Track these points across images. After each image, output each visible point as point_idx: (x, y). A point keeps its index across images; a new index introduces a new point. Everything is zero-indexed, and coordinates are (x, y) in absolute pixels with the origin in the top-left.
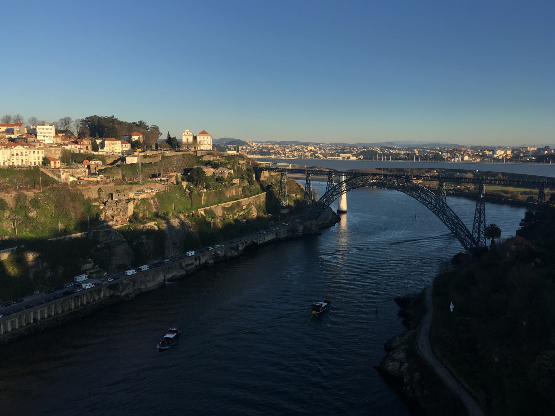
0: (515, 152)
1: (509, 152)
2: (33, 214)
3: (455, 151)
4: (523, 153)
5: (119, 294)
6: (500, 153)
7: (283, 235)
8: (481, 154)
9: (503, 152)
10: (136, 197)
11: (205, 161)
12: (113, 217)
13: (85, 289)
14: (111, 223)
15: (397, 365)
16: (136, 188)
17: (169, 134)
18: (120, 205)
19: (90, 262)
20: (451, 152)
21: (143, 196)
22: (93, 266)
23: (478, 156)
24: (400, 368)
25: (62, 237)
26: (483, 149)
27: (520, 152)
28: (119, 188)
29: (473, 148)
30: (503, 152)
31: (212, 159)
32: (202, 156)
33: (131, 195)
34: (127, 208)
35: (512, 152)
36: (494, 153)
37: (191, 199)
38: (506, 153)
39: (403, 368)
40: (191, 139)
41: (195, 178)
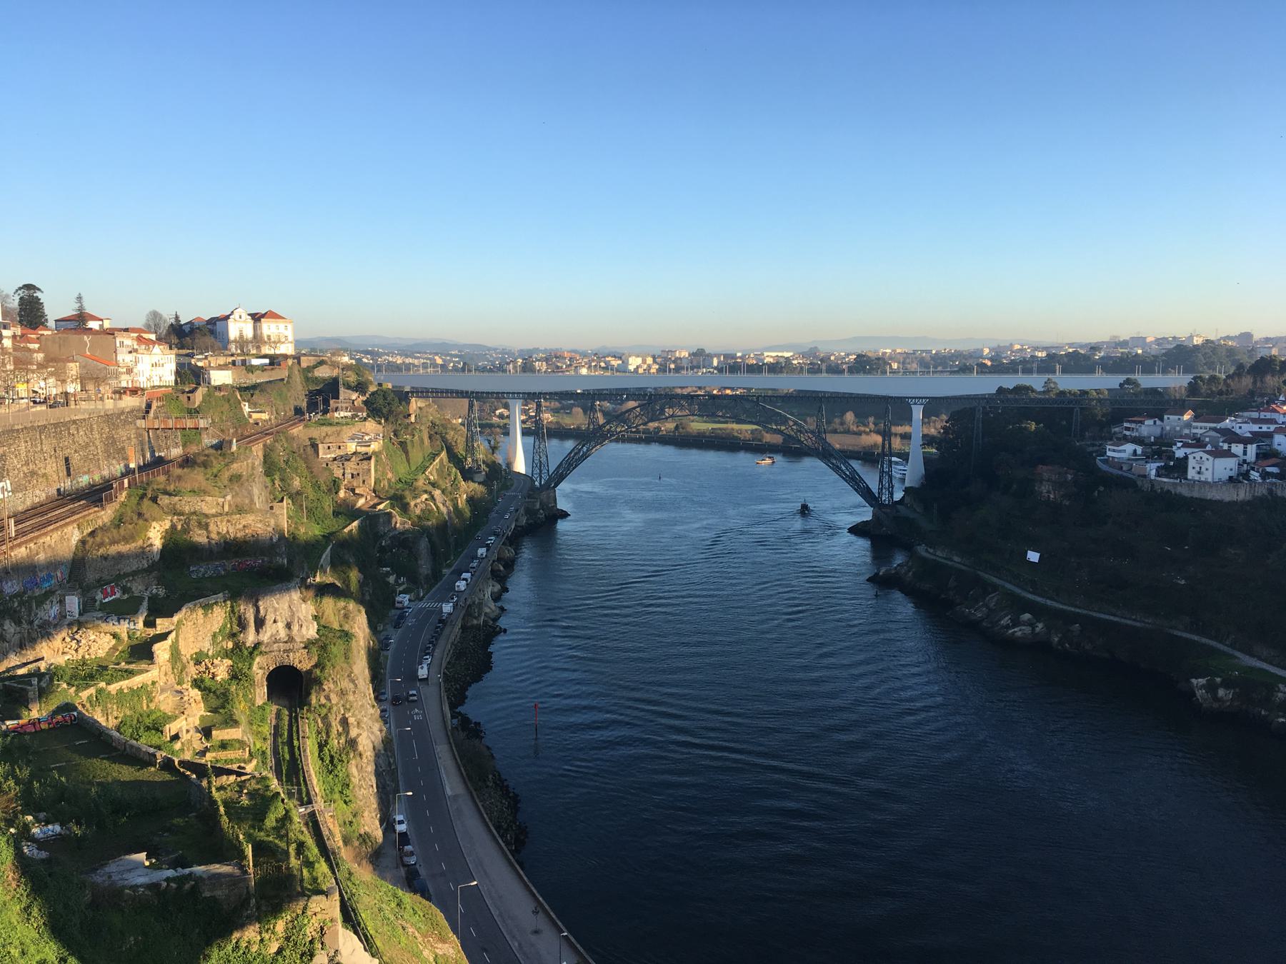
0: (659, 360)
1: (650, 361)
2: (297, 483)
3: (552, 358)
4: (674, 362)
5: (475, 622)
6: (634, 362)
7: (523, 521)
8: (603, 364)
9: (639, 361)
10: (363, 450)
11: (324, 380)
12: (353, 490)
13: (450, 614)
14: (361, 502)
15: (1027, 630)
16: (348, 432)
17: (177, 318)
18: (351, 467)
19: (388, 574)
20: (547, 360)
21: (375, 446)
22: (396, 581)
23: (606, 369)
24: (1033, 629)
25: (349, 528)
26: (599, 356)
27: (666, 359)
28: (316, 433)
29: (584, 355)
30: (639, 361)
31: (335, 373)
32: (310, 369)
33: (352, 447)
34: (369, 470)
35: (655, 362)
36: (625, 363)
37: (406, 453)
38: (644, 361)
39: (1037, 630)
40: (249, 334)
41: (385, 410)
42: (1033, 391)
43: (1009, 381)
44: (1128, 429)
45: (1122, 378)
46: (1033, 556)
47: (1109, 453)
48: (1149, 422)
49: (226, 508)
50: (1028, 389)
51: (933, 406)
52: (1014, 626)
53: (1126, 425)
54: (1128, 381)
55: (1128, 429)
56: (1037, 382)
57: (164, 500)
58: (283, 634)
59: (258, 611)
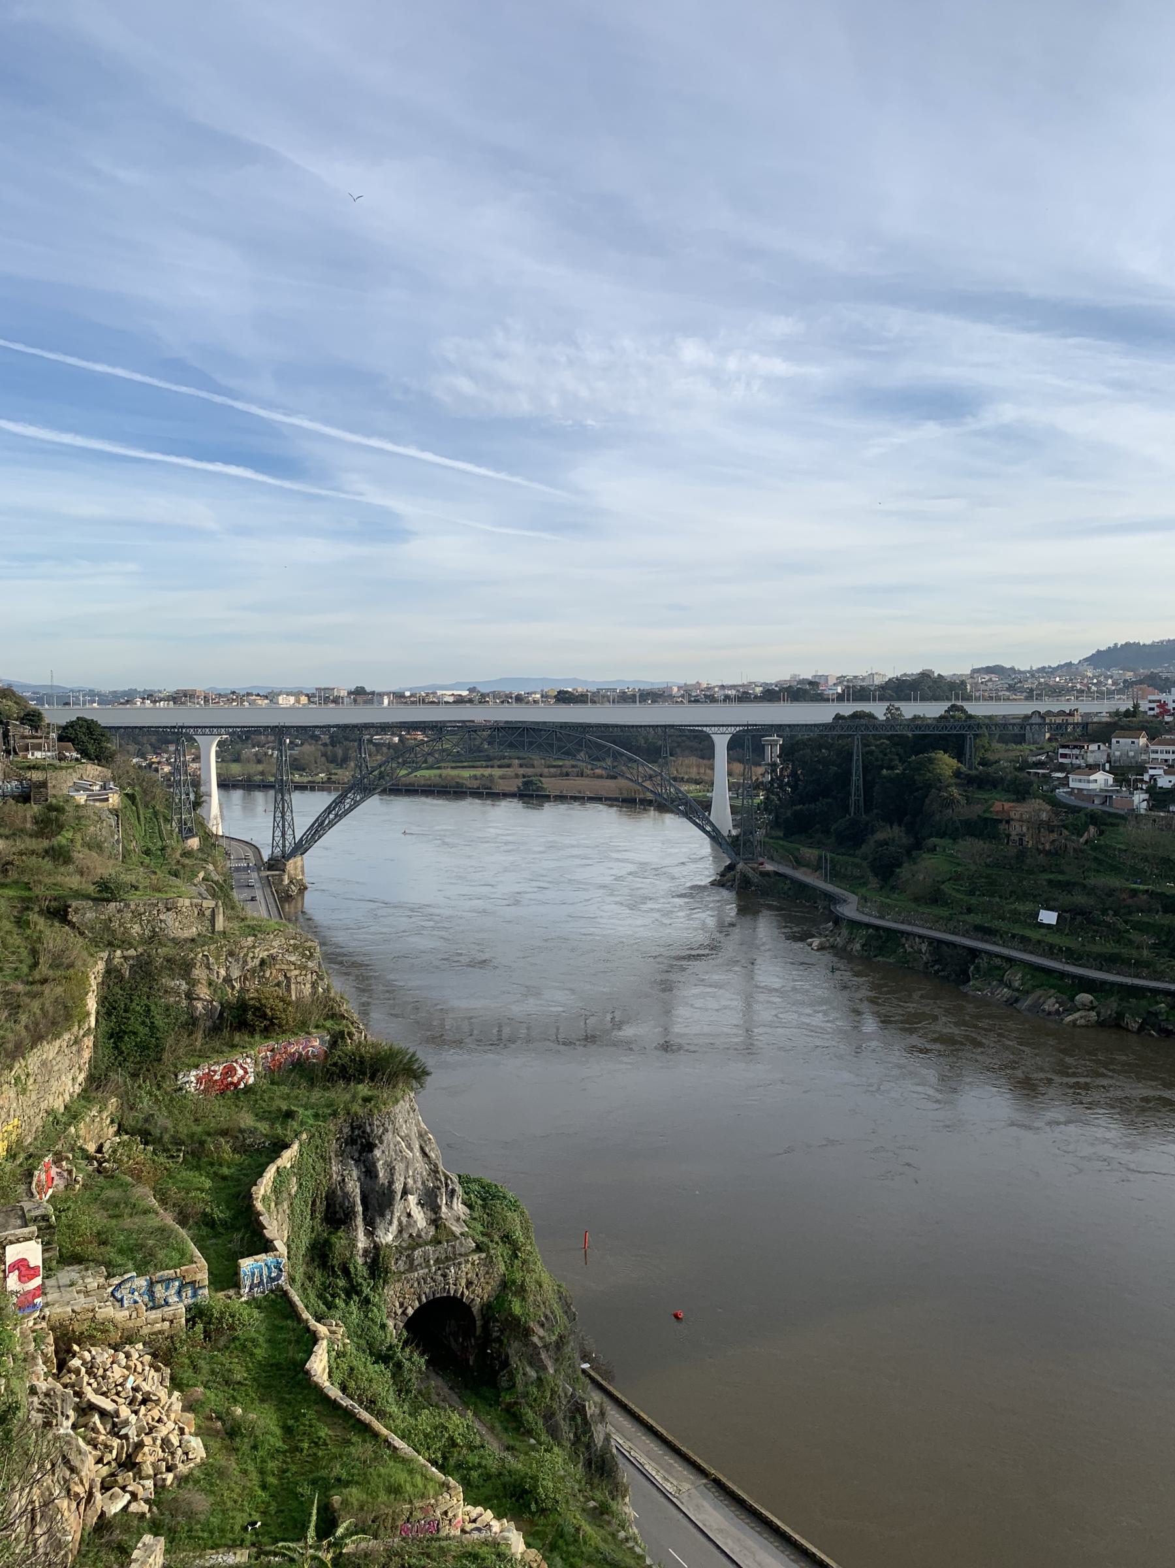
42: (876, 718)
43: (847, 709)
44: (1064, 756)
45: (946, 705)
46: (1048, 917)
47: (1072, 785)
48: (1093, 747)
49: (220, 924)
50: (871, 716)
51: (747, 743)
52: (1069, 1011)
53: (1061, 751)
54: (953, 706)
55: (1064, 756)
56: (879, 710)
57: (86, 914)
58: (420, 1218)
59: (370, 1172)
